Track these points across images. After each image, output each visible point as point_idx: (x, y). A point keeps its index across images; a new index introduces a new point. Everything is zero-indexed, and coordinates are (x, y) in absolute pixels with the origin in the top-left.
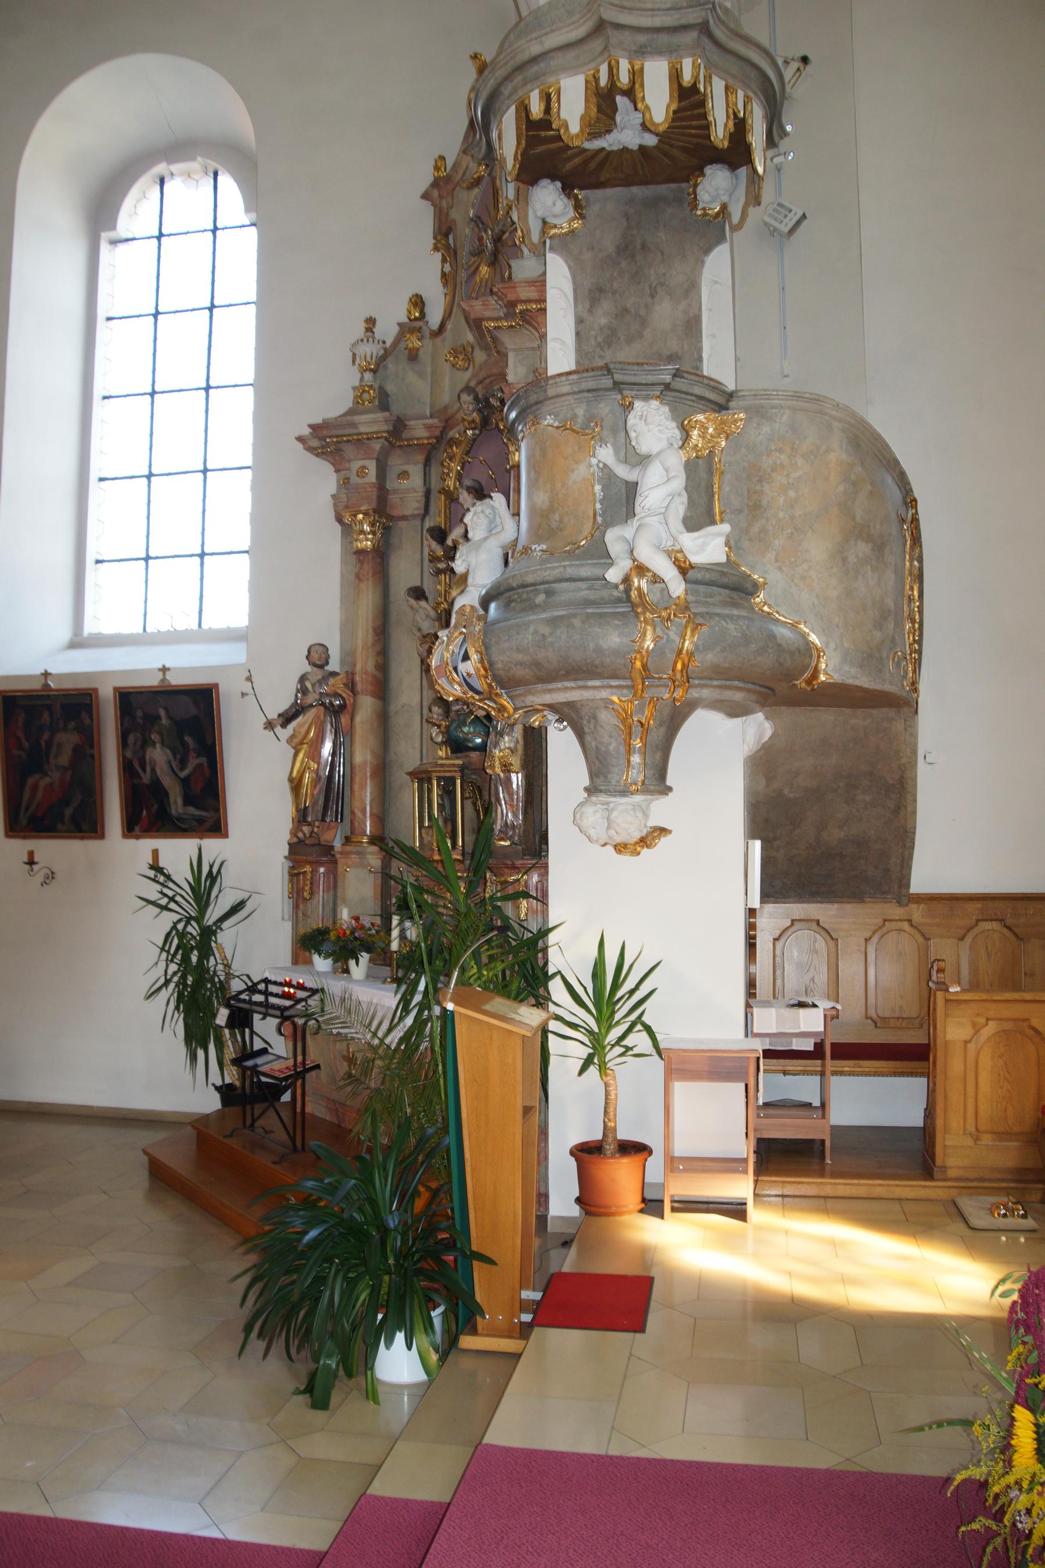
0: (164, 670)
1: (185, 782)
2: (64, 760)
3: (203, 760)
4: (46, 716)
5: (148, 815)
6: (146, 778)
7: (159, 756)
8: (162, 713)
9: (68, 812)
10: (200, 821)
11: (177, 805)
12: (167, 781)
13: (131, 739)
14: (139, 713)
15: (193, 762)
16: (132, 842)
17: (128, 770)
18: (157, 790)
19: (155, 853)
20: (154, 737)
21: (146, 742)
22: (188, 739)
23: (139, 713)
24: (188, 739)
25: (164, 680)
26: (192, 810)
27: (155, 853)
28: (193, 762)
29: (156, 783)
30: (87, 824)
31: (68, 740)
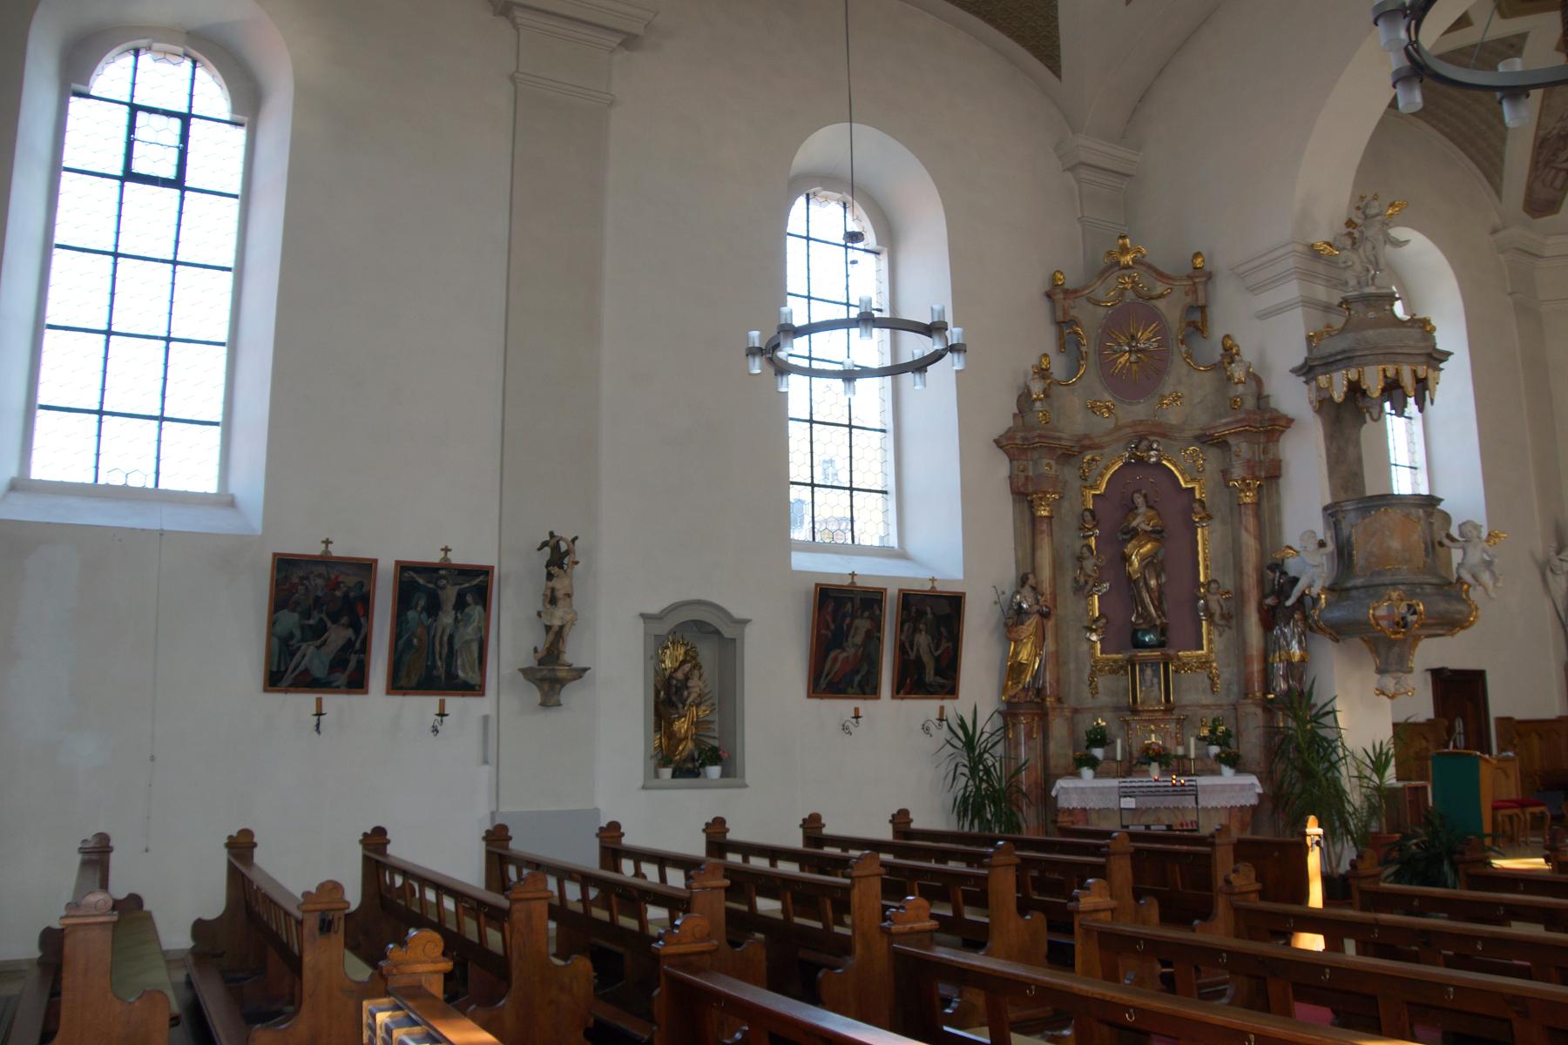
0: (933, 580)
1: (937, 660)
2: (859, 639)
4: (849, 605)
5: (911, 683)
6: (912, 656)
7: (923, 640)
9: (857, 679)
10: (942, 686)
11: (930, 676)
12: (927, 659)
13: (906, 627)
14: (914, 609)
15: (945, 644)
16: (897, 702)
17: (902, 650)
18: (919, 664)
19: (942, 708)
20: (922, 626)
21: (916, 630)
22: (943, 629)
23: (914, 609)
24: (943, 629)
26: (939, 680)
27: (942, 708)
28: (945, 644)
29: (919, 658)
30: (869, 689)
31: (863, 624)
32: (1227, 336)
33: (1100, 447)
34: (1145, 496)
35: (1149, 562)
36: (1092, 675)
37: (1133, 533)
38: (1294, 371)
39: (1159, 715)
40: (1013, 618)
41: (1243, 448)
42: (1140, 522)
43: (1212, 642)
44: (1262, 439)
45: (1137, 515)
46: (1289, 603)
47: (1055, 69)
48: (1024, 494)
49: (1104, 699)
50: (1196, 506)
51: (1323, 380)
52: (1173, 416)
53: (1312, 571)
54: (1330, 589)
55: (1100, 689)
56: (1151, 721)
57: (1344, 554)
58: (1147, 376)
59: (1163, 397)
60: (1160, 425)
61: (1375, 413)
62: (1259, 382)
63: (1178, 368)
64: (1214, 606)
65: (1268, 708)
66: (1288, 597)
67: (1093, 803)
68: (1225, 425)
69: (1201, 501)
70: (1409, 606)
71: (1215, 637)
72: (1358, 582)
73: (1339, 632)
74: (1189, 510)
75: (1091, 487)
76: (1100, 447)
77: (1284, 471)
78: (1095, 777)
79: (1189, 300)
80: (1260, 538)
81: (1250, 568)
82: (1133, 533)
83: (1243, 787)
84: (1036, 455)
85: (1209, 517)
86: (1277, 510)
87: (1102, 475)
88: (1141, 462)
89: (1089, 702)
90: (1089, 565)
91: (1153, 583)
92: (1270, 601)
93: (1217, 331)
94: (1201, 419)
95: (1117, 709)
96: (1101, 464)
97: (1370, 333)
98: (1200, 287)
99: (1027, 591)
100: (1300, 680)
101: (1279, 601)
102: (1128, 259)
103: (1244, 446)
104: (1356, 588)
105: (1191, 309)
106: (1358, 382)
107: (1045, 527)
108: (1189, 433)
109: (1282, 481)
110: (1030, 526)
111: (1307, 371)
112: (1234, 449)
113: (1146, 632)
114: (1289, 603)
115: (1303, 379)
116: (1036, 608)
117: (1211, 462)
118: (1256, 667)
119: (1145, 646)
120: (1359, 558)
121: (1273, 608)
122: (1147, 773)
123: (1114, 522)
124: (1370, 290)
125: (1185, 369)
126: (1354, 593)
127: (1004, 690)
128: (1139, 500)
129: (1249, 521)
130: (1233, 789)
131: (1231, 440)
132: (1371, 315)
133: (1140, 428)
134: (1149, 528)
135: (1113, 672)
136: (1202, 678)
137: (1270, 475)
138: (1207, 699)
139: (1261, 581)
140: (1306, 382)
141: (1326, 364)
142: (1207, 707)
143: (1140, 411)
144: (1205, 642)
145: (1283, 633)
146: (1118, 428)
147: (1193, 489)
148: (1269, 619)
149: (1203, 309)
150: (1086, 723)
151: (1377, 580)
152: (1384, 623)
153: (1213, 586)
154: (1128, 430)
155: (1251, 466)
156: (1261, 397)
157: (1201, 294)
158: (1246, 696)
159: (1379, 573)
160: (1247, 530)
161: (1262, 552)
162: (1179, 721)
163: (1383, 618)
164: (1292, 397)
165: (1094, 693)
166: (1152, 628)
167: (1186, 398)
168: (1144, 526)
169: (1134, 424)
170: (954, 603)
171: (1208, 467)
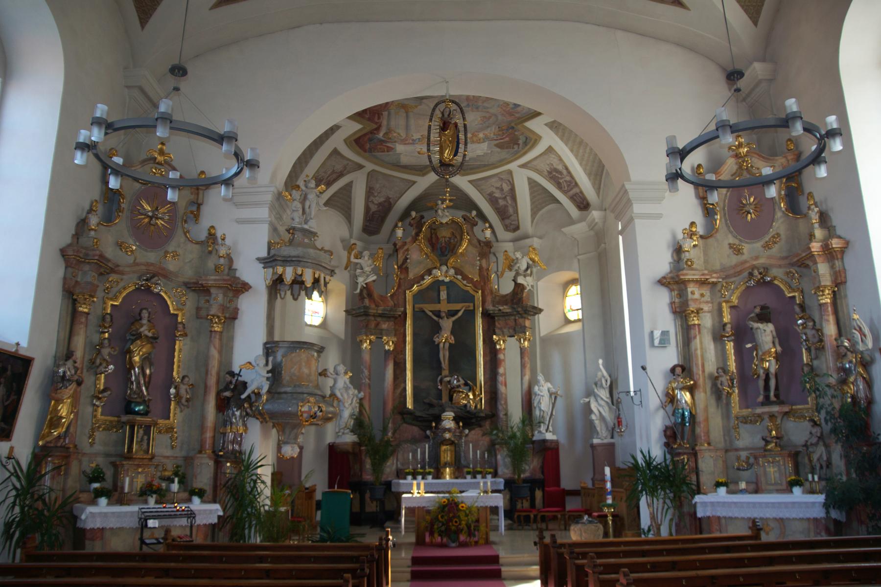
3: (15, 397)
8: (9, 367)
22: (14, 384)
24: (14, 384)
25: (17, 350)
28: (13, 397)
32: (212, 227)
33: (122, 273)
34: (149, 313)
35: (147, 360)
36: (93, 430)
37: (139, 336)
38: (258, 259)
39: (146, 462)
40: (55, 384)
41: (218, 297)
42: (145, 330)
43: (176, 416)
44: (231, 294)
45: (142, 326)
46: (243, 397)
47: (143, 22)
48: (71, 295)
49: (98, 448)
50: (180, 326)
51: (280, 270)
52: (171, 265)
53: (257, 380)
54: (269, 392)
55: (97, 441)
56: (139, 466)
57: (275, 374)
58: (150, 235)
59: (167, 252)
60: (164, 269)
61: (283, 294)
62: (230, 260)
63: (179, 237)
64: (183, 391)
65: (218, 463)
66: (243, 393)
67: (112, 523)
68: (215, 280)
69: (182, 323)
70: (319, 407)
71: (178, 410)
72: (289, 389)
73: (260, 416)
74: (172, 329)
75: (111, 299)
76: (122, 273)
77: (239, 316)
78: (109, 504)
79: (192, 197)
80: (220, 352)
81: (214, 371)
82: (139, 336)
83: (211, 511)
84: (87, 268)
85: (186, 335)
86: (231, 339)
87: (121, 293)
88: (148, 290)
89: (87, 449)
90: (105, 352)
91: (148, 372)
92: (227, 394)
93: (206, 221)
94: (188, 274)
95: (107, 455)
96: (121, 284)
97: (312, 251)
98: (201, 192)
99: (70, 363)
100: (240, 444)
101: (233, 394)
102: (160, 159)
103: (220, 298)
104: (286, 393)
105: (193, 203)
106: (301, 275)
107: (83, 320)
108: (181, 280)
109: (237, 321)
110: (73, 316)
111: (268, 261)
112: (213, 296)
113: (139, 404)
114: (243, 397)
115: (262, 265)
116: (76, 377)
117: (191, 300)
118: (209, 435)
119: (138, 413)
120: (286, 377)
121: (228, 399)
122: (146, 502)
123: (125, 328)
124: (306, 227)
125: (182, 239)
126: (284, 396)
127: (38, 436)
128: (145, 314)
129: (217, 342)
130: (208, 512)
131: (213, 291)
132: (306, 240)
133: (151, 268)
134: (150, 335)
135: (107, 429)
136: (165, 438)
137: (231, 316)
138: (169, 453)
139: (218, 382)
140: (264, 268)
141: (283, 261)
142: (168, 457)
143: (152, 257)
144: (171, 415)
145: (233, 414)
146: (136, 264)
147: (177, 315)
148: (223, 405)
149: (199, 206)
150: (89, 466)
151: (299, 390)
152: (305, 415)
153: (186, 379)
154: (143, 267)
155: (224, 308)
156: (231, 269)
157: (201, 196)
158: (200, 452)
159: (299, 386)
160: (215, 347)
161: (220, 363)
162: (157, 466)
163: (305, 412)
164: (255, 275)
165: (92, 445)
166: (144, 402)
167: (181, 259)
168: (146, 333)
169: (148, 264)
170: (27, 362)
171: (188, 303)
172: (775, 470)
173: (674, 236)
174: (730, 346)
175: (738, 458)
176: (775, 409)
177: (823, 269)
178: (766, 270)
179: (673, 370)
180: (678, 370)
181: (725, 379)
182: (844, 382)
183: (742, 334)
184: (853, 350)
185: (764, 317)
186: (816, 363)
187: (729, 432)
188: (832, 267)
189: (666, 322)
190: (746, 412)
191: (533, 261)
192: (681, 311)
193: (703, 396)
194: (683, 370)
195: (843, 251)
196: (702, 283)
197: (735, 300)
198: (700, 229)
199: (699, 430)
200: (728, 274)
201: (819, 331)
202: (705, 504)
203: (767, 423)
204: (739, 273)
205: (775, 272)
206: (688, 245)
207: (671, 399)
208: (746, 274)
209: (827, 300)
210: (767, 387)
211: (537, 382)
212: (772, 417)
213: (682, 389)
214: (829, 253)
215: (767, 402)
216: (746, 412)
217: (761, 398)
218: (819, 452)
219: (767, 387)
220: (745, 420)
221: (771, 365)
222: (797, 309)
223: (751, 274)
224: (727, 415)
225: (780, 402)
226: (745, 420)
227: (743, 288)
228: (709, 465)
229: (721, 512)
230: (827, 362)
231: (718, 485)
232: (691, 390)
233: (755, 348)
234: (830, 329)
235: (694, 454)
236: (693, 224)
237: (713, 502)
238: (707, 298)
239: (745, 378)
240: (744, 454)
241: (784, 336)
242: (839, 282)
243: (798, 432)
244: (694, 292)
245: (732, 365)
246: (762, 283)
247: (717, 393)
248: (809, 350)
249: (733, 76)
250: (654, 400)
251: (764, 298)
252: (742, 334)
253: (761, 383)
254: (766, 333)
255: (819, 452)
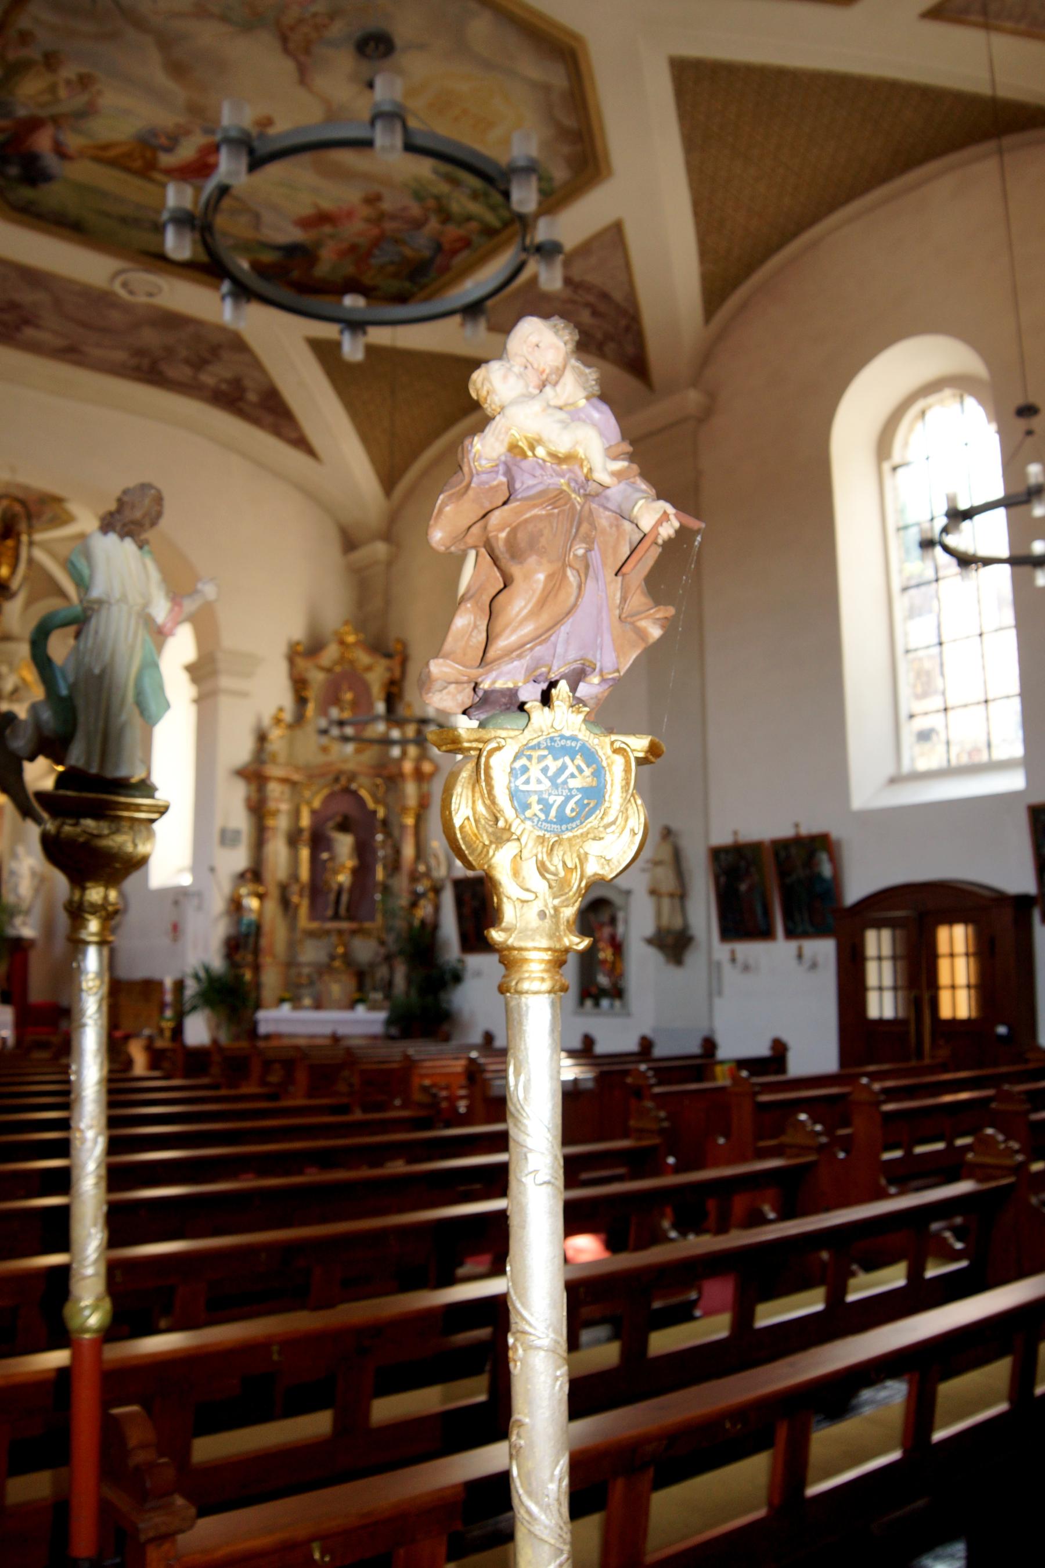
172: (337, 988)
173: (259, 720)
174: (305, 853)
175: (299, 975)
176: (345, 925)
177: (411, 789)
178: (352, 777)
179: (242, 876)
180: (249, 876)
181: (295, 888)
182: (414, 905)
183: (319, 841)
184: (428, 874)
185: (344, 827)
186: (390, 882)
187: (292, 946)
188: (420, 788)
189: (240, 820)
190: (315, 925)
191: (24, 680)
192: (258, 810)
193: (272, 907)
194: (254, 874)
195: (432, 775)
196: (284, 781)
197: (317, 804)
198: (288, 716)
199: (264, 942)
200: (313, 775)
201: (397, 851)
202: (267, 1021)
203: (334, 939)
204: (323, 775)
205: (363, 780)
206: (276, 734)
207: (236, 906)
208: (331, 777)
209: (410, 821)
210: (337, 902)
211: (14, 855)
212: (340, 932)
213: (250, 894)
214: (419, 776)
215: (336, 916)
216: (315, 925)
217: (330, 912)
218: (382, 972)
219: (337, 902)
220: (311, 934)
221: (343, 878)
222: (378, 825)
223: (337, 779)
224: (292, 926)
225: (351, 917)
226: (311, 934)
227: (325, 792)
228: (271, 979)
229: (284, 1029)
230: (401, 883)
231: (282, 1000)
232: (261, 897)
233: (332, 858)
234: (408, 851)
235: (257, 968)
236: (281, 709)
237: (277, 1019)
238: (287, 795)
239: (316, 889)
240: (306, 970)
241: (363, 851)
242: (424, 804)
243: (365, 950)
244: (274, 789)
245: (304, 873)
246: (347, 791)
247: (285, 903)
248: (385, 867)
249: (349, 543)
250: (218, 904)
251: (345, 806)
252: (319, 841)
253: (332, 897)
254: (344, 844)
255: (382, 972)
